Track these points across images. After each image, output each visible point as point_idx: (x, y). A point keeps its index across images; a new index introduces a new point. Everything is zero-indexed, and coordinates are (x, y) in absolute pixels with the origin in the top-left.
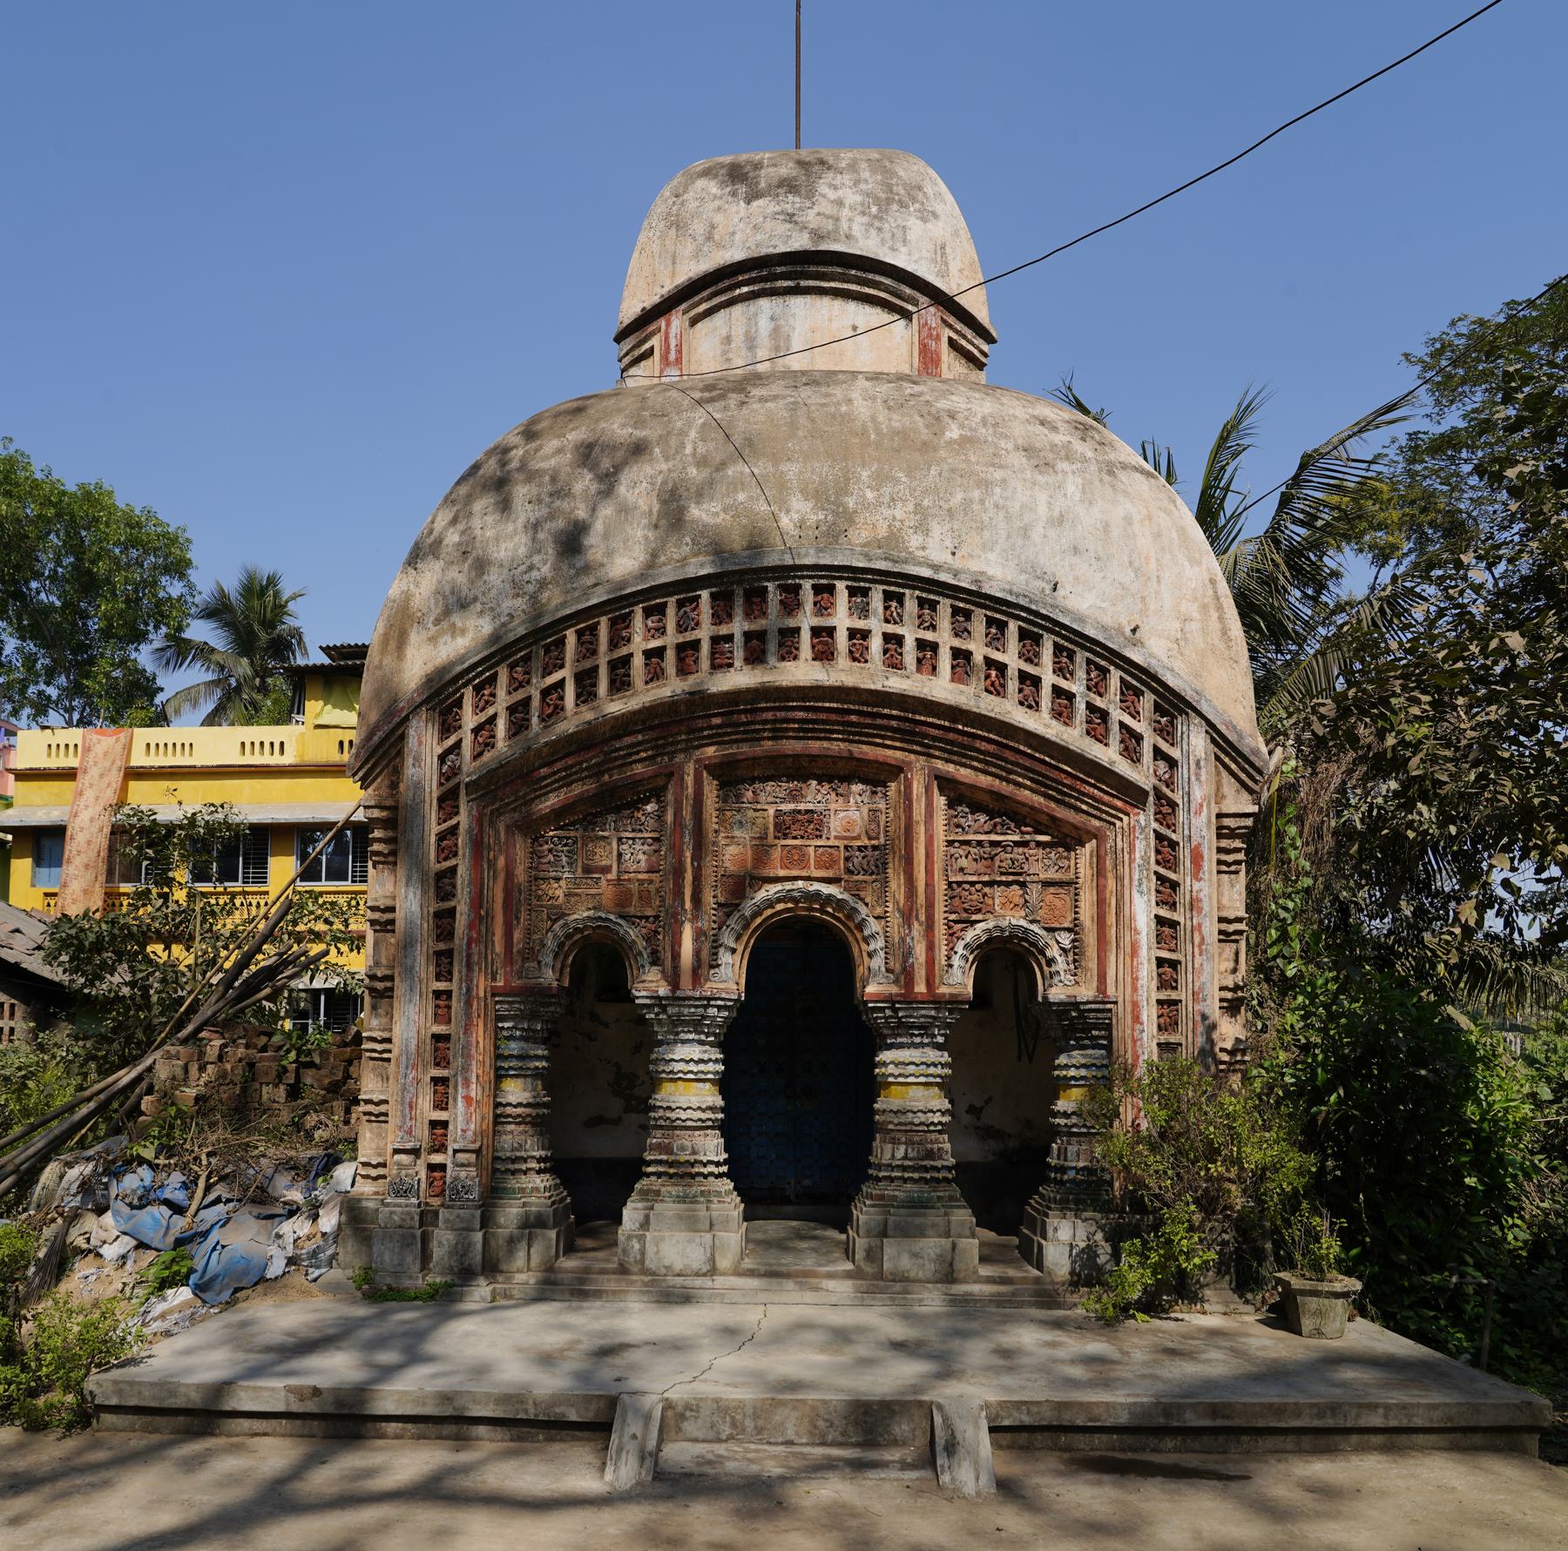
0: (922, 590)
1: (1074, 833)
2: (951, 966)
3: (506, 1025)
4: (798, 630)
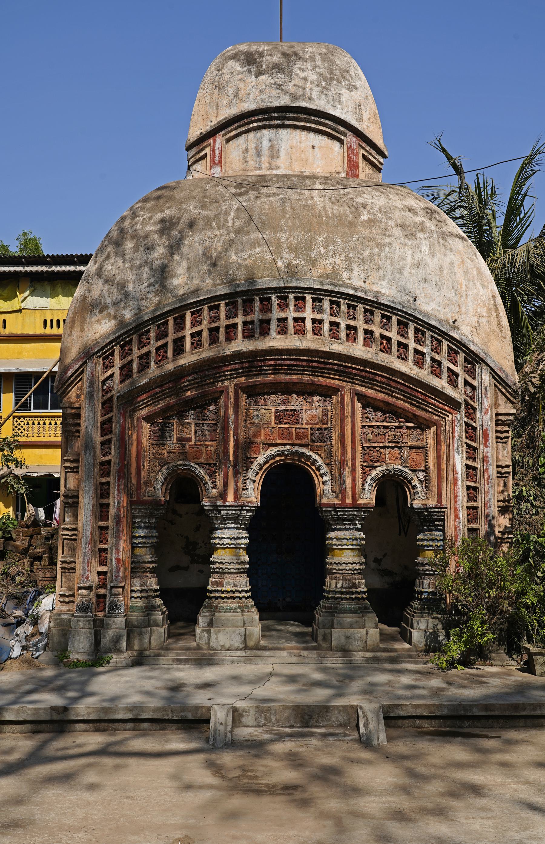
0: (349, 300)
1: (425, 422)
2: (364, 489)
3: (137, 520)
4: (286, 319)
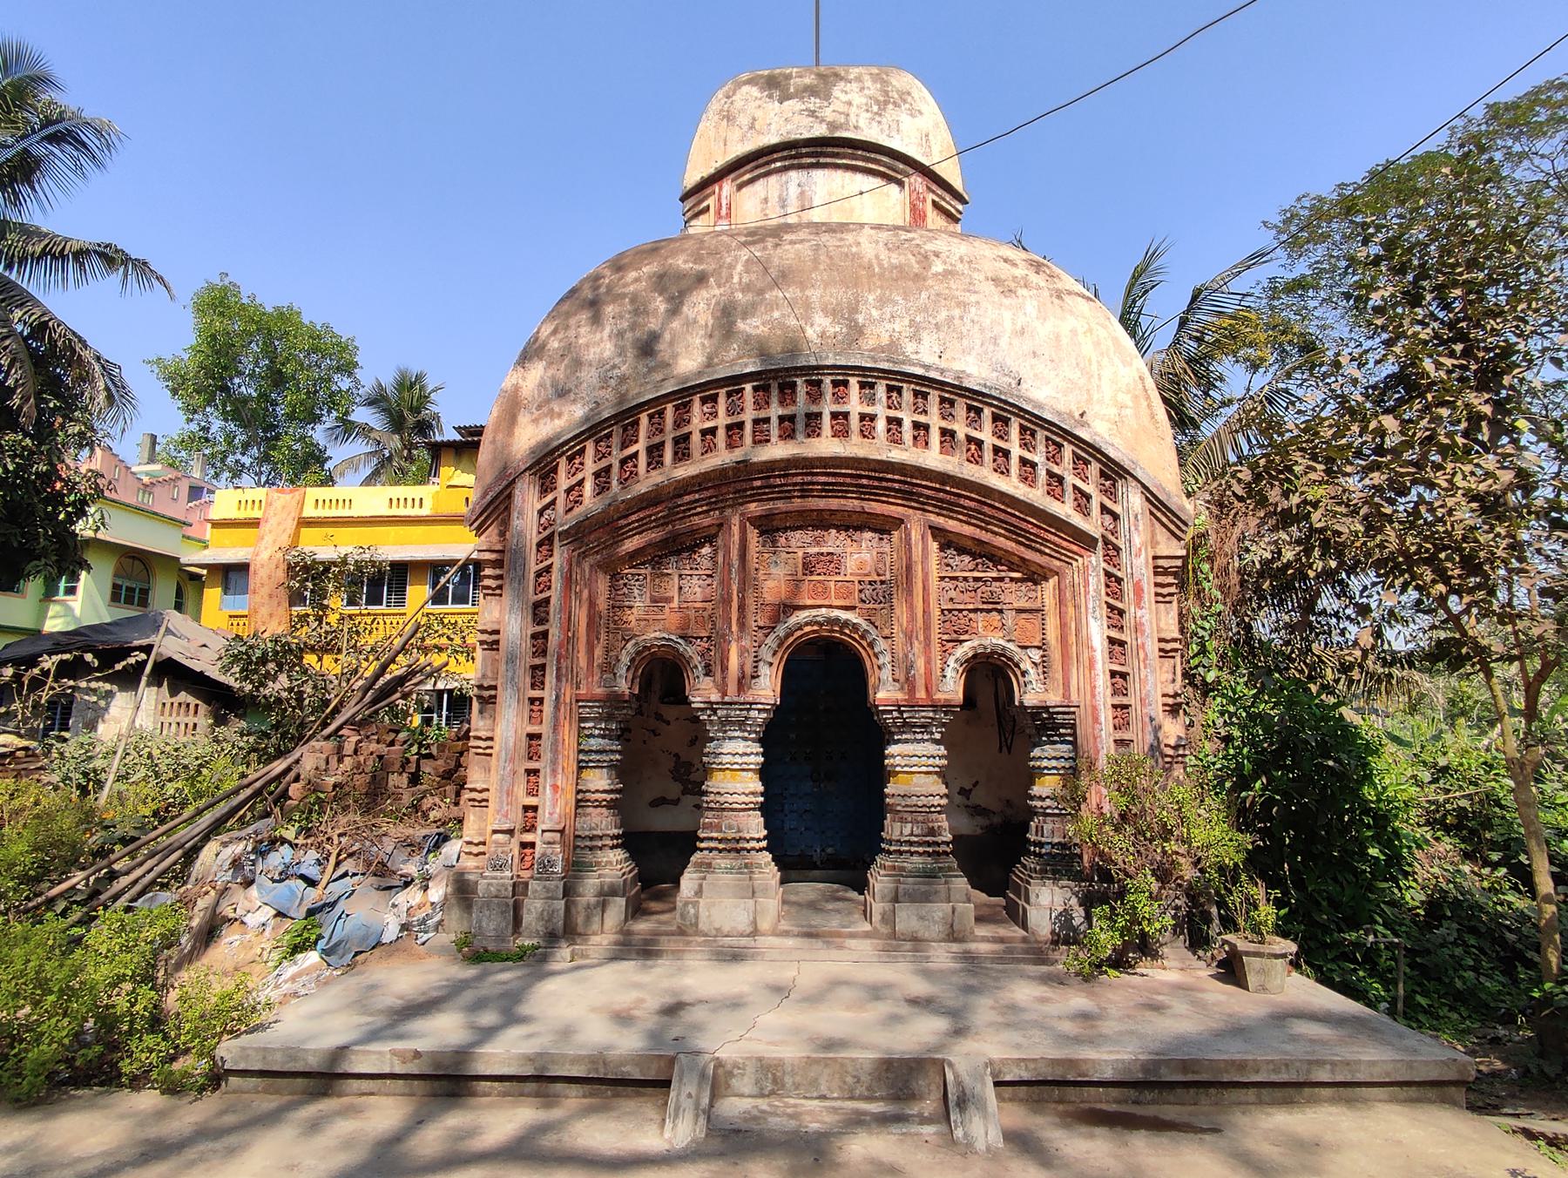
1: (1040, 571)
